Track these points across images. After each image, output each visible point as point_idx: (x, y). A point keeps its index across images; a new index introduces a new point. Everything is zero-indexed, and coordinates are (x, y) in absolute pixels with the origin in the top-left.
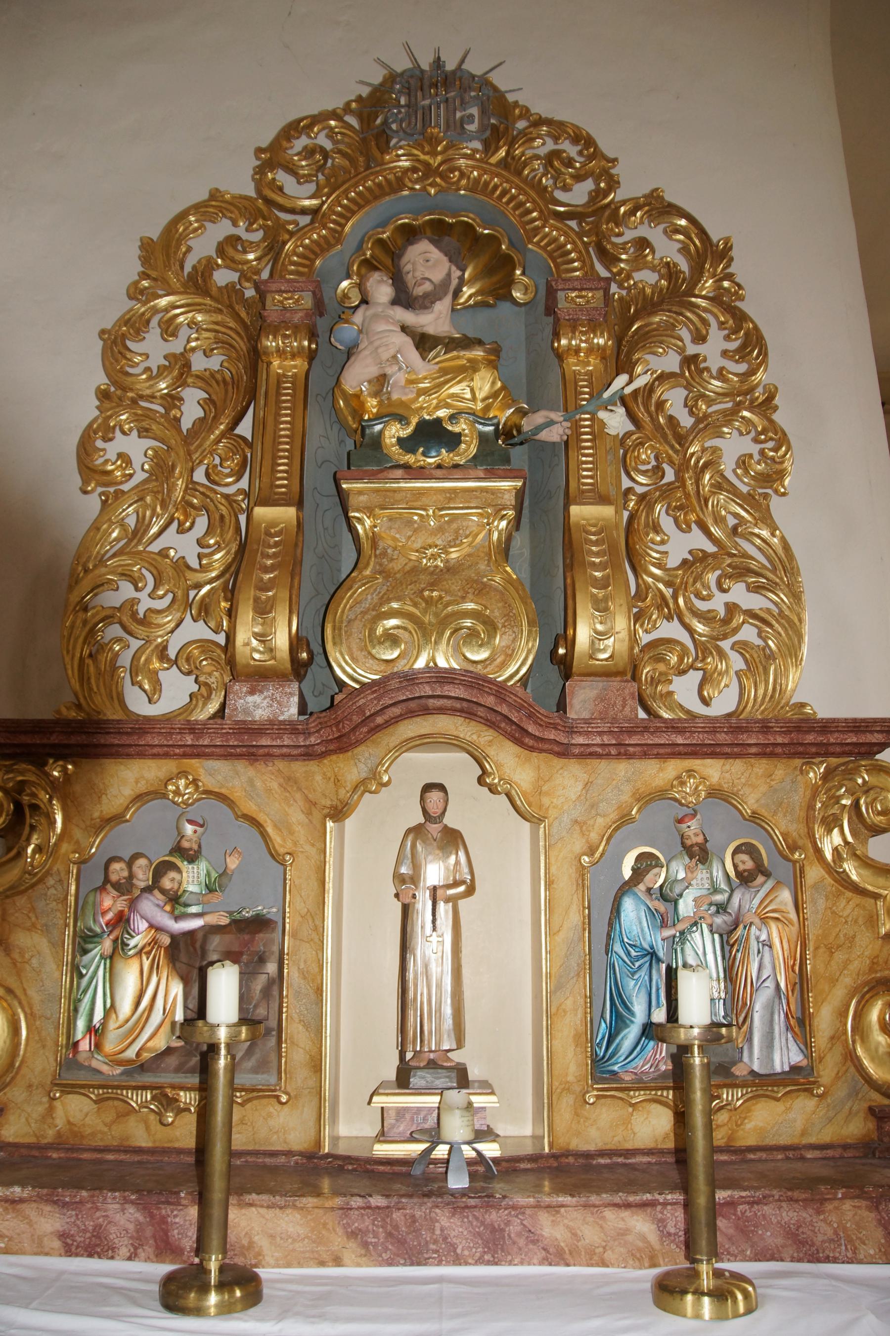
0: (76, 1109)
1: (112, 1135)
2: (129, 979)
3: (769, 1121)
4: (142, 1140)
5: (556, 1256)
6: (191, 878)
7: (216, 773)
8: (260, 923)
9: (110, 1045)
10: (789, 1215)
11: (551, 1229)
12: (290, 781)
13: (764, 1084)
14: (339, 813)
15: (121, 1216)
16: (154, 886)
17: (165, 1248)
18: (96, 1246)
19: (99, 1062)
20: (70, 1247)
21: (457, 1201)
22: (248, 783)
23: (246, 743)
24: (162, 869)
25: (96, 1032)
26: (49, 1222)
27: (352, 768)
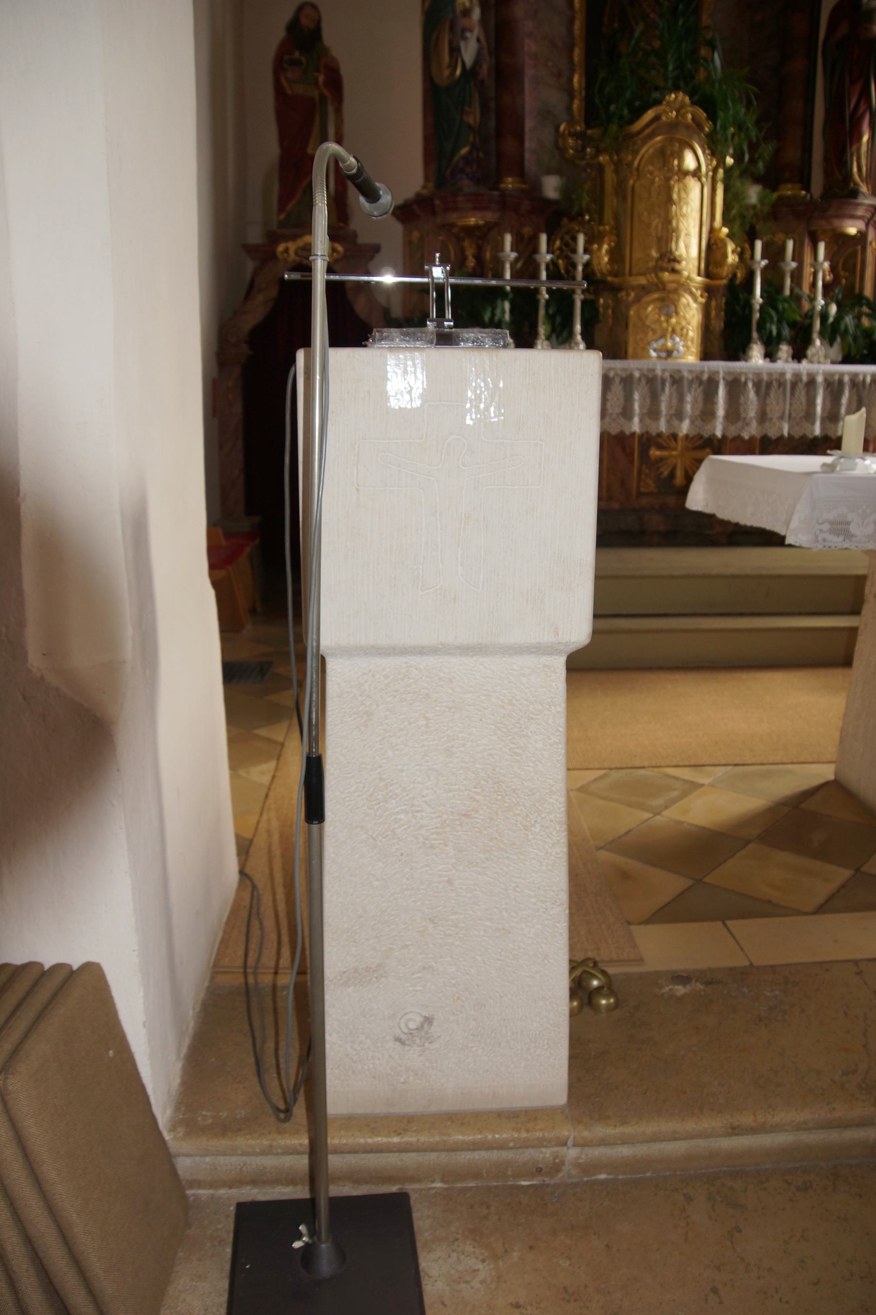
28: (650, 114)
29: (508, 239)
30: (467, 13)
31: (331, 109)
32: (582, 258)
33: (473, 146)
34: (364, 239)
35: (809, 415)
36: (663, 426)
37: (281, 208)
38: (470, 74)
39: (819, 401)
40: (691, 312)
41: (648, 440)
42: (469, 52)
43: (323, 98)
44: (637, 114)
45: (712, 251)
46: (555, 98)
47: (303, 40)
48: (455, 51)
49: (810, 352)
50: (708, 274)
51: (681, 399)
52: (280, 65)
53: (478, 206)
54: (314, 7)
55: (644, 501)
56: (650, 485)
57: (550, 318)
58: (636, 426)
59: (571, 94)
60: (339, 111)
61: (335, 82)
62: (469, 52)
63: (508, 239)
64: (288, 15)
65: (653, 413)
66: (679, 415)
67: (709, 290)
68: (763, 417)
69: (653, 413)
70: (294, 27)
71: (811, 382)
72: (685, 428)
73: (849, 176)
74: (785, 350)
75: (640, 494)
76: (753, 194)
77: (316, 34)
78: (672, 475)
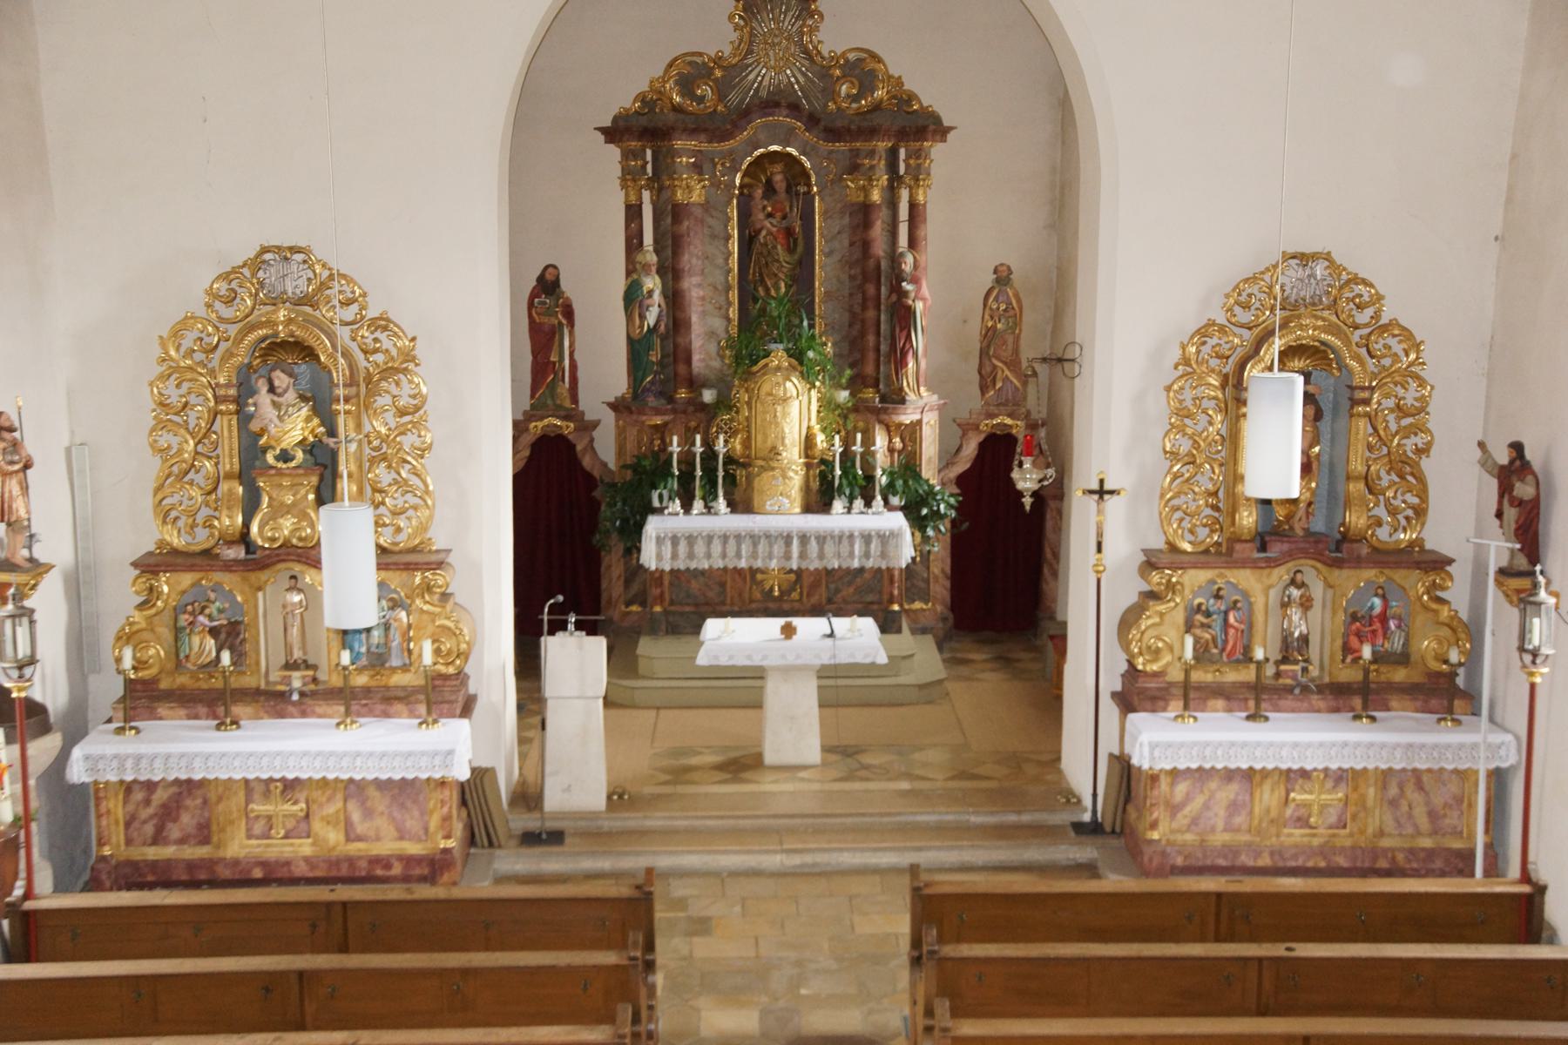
0: (182, 680)
1: (197, 685)
2: (196, 640)
3: (399, 679)
4: (205, 686)
5: (320, 716)
6: (213, 609)
7: (218, 576)
8: (237, 623)
9: (192, 657)
10: (383, 707)
11: (319, 710)
12: (245, 579)
13: (394, 670)
14: (259, 589)
15: (202, 710)
16: (201, 613)
17: (215, 717)
18: (196, 717)
19: (189, 665)
20: (189, 717)
21: (294, 704)
22: (228, 580)
23: (229, 566)
24: (204, 608)
25: (187, 657)
26: (183, 712)
27: (263, 576)
28: (763, 362)
29: (675, 439)
30: (650, 293)
31: (566, 332)
32: (720, 447)
33: (656, 373)
34: (589, 417)
35: (852, 554)
36: (759, 564)
37: (532, 396)
38: (653, 330)
39: (857, 547)
40: (796, 479)
41: (753, 572)
42: (651, 317)
43: (560, 324)
44: (755, 362)
45: (809, 441)
46: (718, 323)
47: (548, 285)
48: (642, 317)
49: (874, 503)
50: (807, 456)
51: (771, 545)
52: (531, 305)
53: (658, 412)
54: (555, 267)
55: (754, 606)
56: (757, 595)
57: (703, 487)
58: (743, 564)
59: (729, 320)
60: (571, 333)
61: (569, 313)
62: (651, 317)
63: (675, 439)
64: (538, 273)
65: (754, 555)
66: (770, 557)
67: (808, 466)
68: (821, 556)
69: (754, 555)
70: (541, 279)
71: (851, 536)
72: (774, 564)
73: (901, 389)
74: (859, 503)
75: (751, 601)
76: (843, 396)
77: (556, 283)
78: (772, 589)
